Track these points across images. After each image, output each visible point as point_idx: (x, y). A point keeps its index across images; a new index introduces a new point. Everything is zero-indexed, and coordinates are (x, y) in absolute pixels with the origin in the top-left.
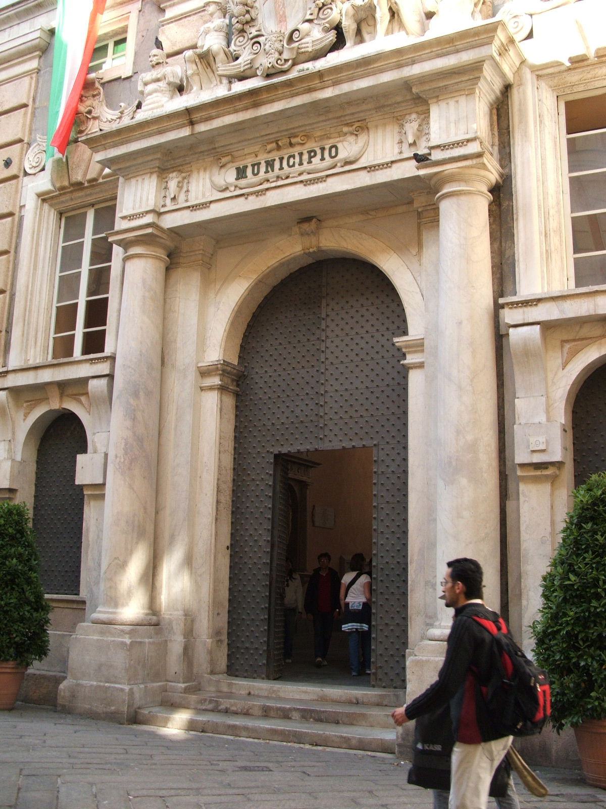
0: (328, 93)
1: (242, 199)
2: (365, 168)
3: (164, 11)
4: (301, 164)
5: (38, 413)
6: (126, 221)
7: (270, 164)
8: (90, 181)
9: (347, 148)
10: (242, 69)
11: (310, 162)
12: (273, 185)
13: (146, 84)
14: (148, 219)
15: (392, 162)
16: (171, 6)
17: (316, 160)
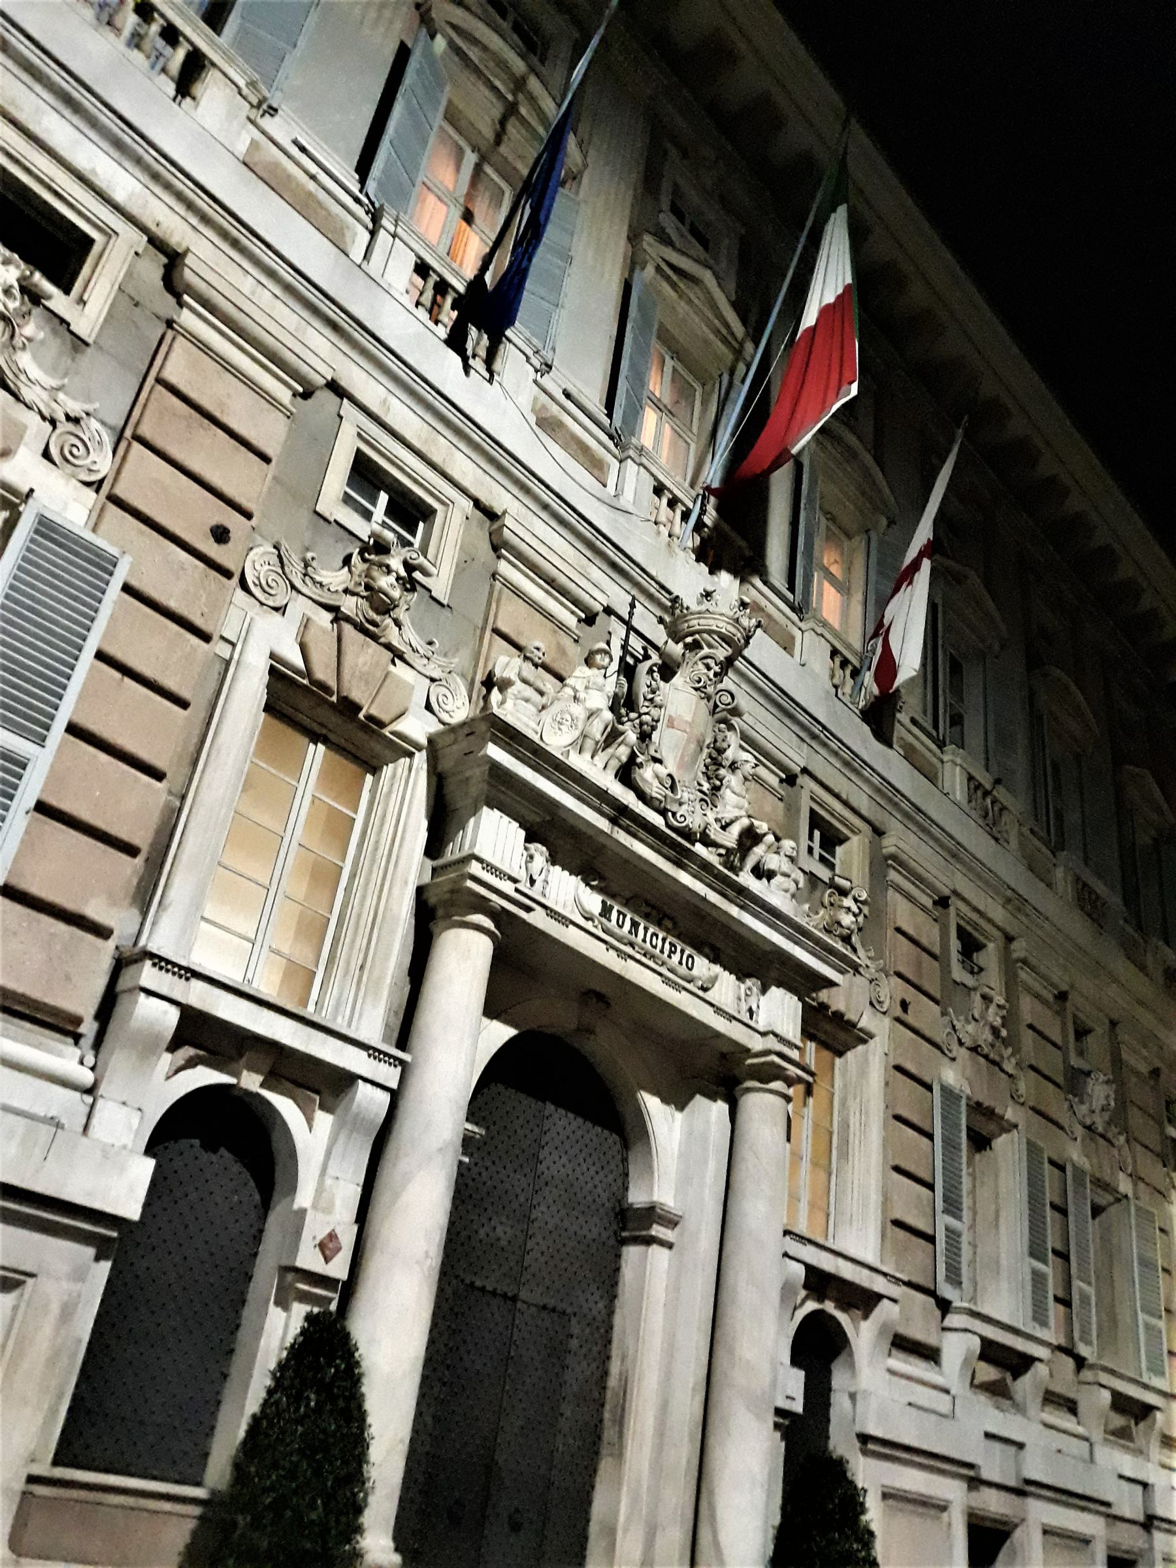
0: (734, 911)
1: (604, 946)
2: (712, 1005)
3: (499, 557)
4: (662, 951)
5: (205, 1076)
6: (480, 865)
7: (635, 925)
8: (370, 718)
9: (703, 967)
10: (654, 795)
11: (669, 956)
12: (638, 956)
13: (525, 681)
14: (507, 887)
15: (735, 1018)
16: (510, 562)
17: (676, 958)
